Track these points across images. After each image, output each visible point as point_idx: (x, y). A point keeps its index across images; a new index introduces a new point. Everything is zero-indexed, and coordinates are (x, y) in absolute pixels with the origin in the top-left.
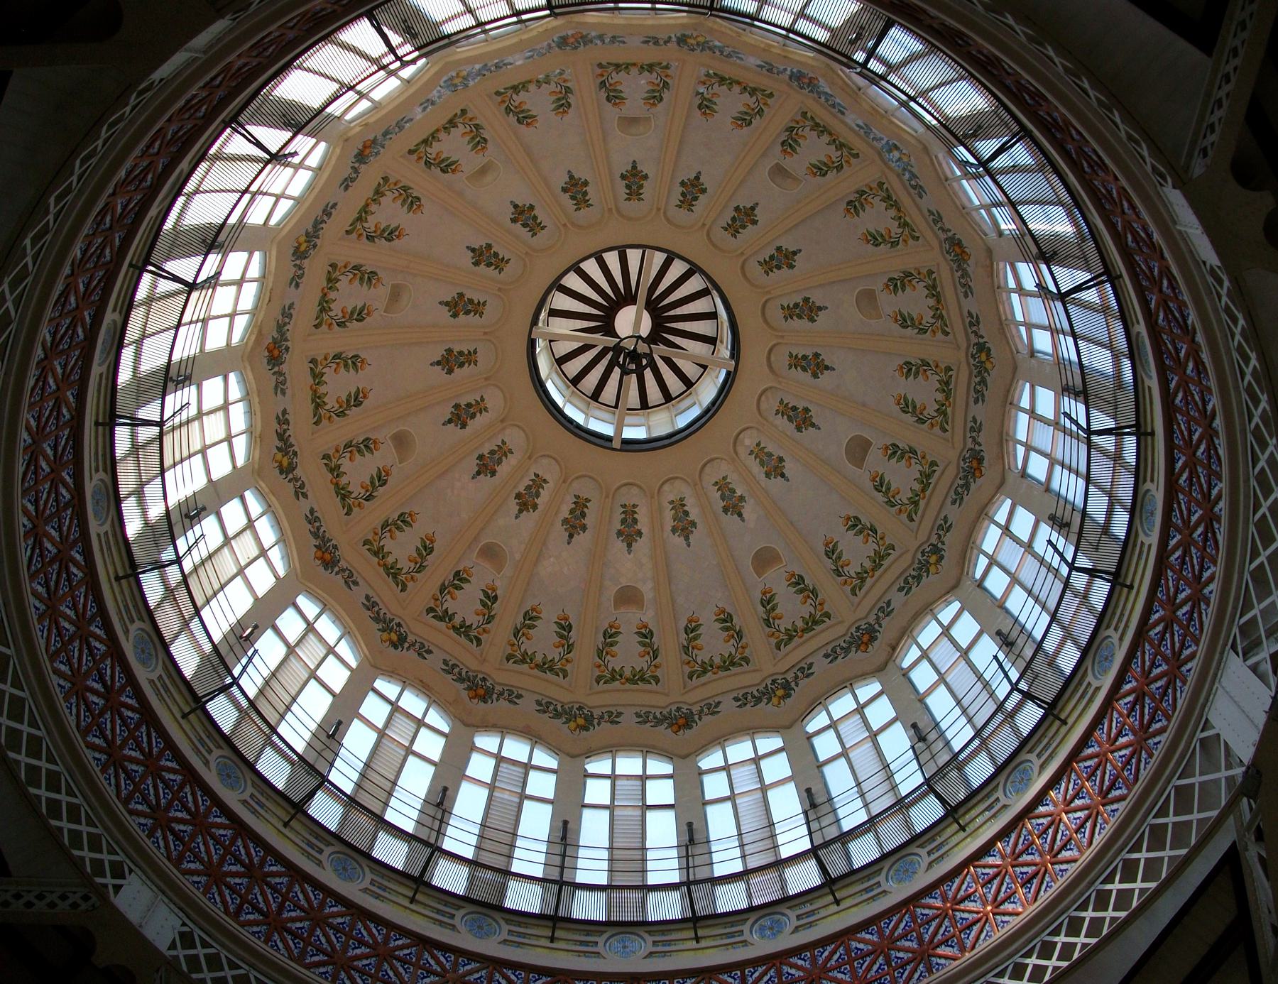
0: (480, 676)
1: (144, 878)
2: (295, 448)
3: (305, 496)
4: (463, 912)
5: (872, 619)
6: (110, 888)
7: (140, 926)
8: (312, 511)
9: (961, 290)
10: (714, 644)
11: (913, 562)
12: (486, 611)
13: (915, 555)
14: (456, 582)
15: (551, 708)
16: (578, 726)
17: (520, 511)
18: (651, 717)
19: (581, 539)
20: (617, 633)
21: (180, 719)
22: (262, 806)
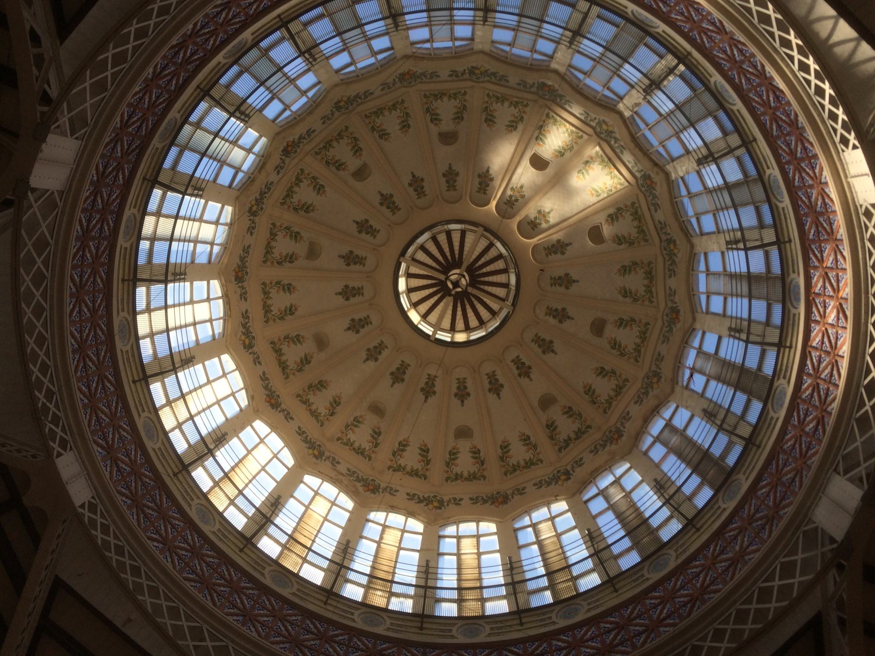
2: (432, 495)
3: (461, 500)
4: (720, 500)
8: (471, 499)
9: (434, 79)
14: (552, 429)
16: (657, 383)
17: (529, 377)
19: (557, 346)
21: (522, 628)
22: (598, 600)
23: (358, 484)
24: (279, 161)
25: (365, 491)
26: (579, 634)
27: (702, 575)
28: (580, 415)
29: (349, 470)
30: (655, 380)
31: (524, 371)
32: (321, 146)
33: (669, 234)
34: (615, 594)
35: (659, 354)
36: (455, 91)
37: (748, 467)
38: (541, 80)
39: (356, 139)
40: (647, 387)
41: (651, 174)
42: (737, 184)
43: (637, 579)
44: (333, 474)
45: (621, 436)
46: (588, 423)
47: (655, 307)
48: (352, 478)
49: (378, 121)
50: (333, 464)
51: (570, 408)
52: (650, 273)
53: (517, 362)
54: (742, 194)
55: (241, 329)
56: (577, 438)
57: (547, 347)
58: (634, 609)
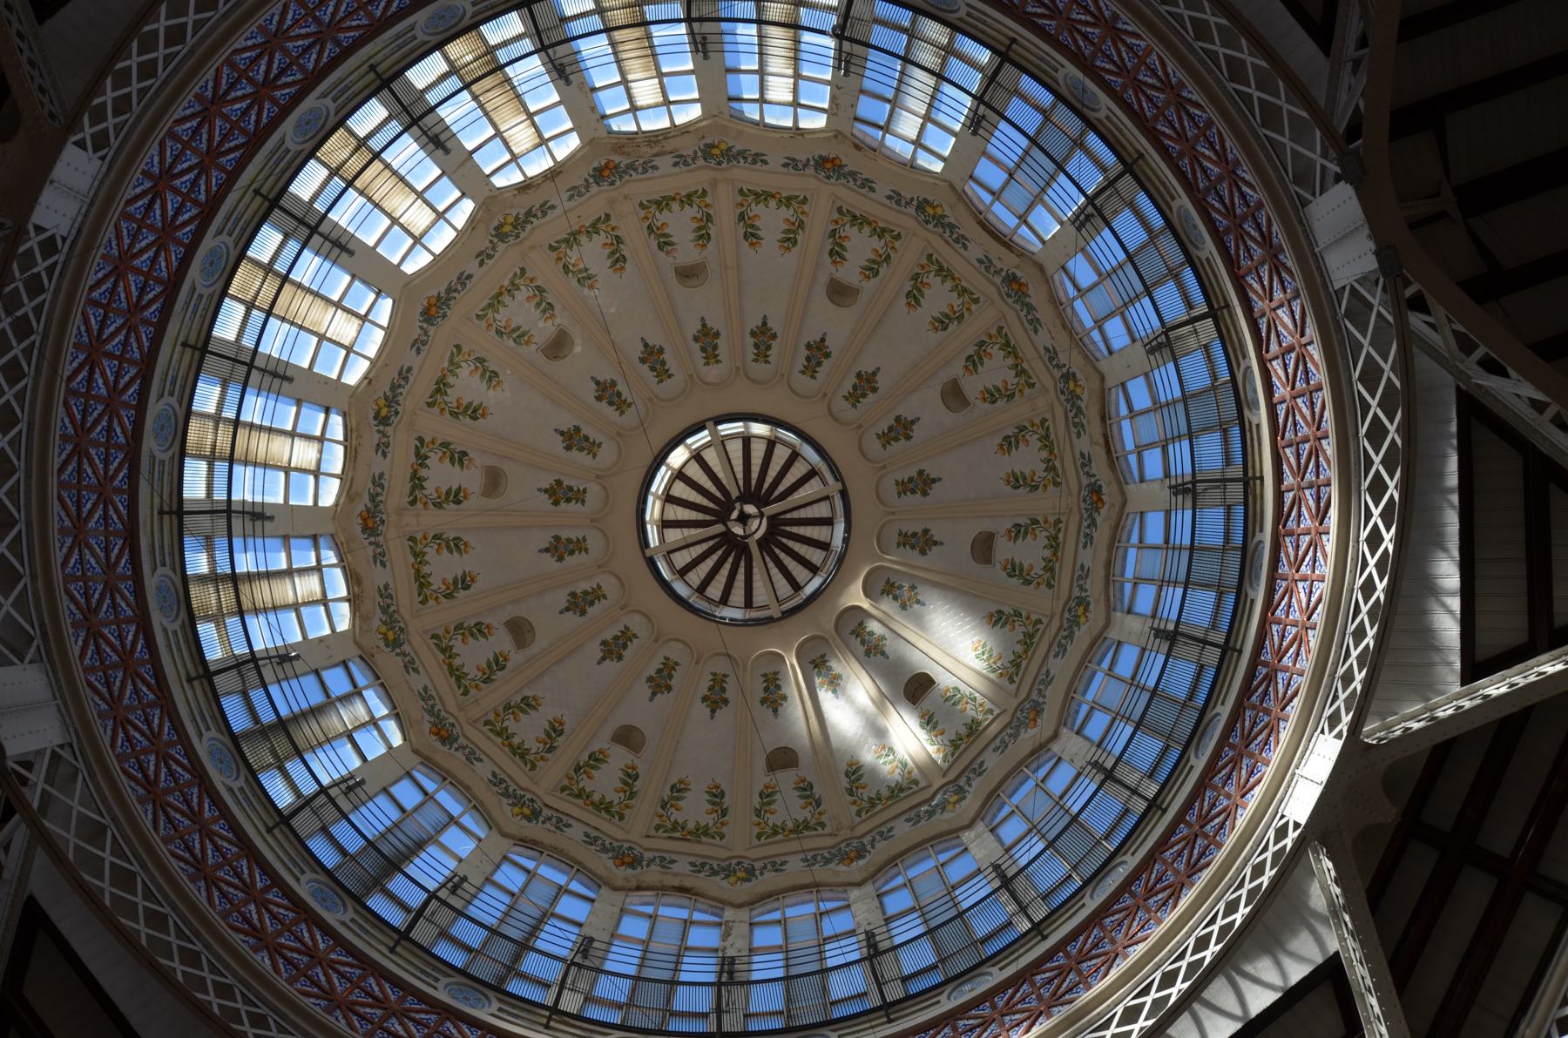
0: (384, 517)
1: (100, 176)
3: (482, 264)
5: (648, 855)
6: (79, 136)
7: (52, 182)
8: (470, 277)
11: (724, 860)
12: (443, 497)
13: (731, 858)
15: (388, 601)
16: (385, 634)
17: (546, 491)
18: (431, 702)
19: (549, 562)
20: (485, 636)
22: (194, 313)
23: (625, 161)
24: (1094, 471)
25: (609, 162)
26: (175, 253)
27: (101, 466)
28: (438, 505)
29: (655, 168)
30: (391, 635)
32: (1061, 536)
33: (543, 822)
34: (181, 339)
37: (178, 643)
38: (868, 857)
39: (1027, 582)
40: (391, 619)
41: (635, 872)
42: (517, 958)
43: (174, 382)
44: (669, 145)
45: (365, 529)
46: (419, 505)
48: (641, 161)
50: (681, 156)
51: (458, 502)
52: (522, 756)
53: (578, 496)
54: (503, 951)
55: (952, 220)
56: (414, 475)
58: (140, 347)
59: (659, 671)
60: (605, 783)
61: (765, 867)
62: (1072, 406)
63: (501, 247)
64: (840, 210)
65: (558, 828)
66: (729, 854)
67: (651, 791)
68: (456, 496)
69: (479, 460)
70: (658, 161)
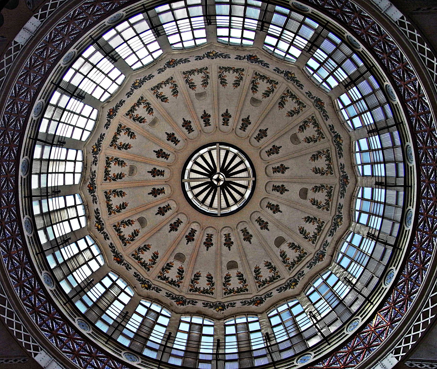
3: (108, 239)
8: (111, 244)
10: (266, 274)
11: (332, 224)
29: (95, 171)
30: (220, 308)
31: (190, 238)
32: (261, 74)
33: (299, 280)
35: (235, 303)
36: (322, 132)
47: (258, 290)
49: (288, 98)
50: (93, 162)
57: (208, 243)
59: (260, 224)
60: (292, 255)
61: (339, 211)
62: (218, 57)
63: (105, 230)
64: (127, 115)
65: (302, 276)
66: (330, 222)
67: (299, 240)
68: (181, 271)
69: (171, 260)
70: (93, 170)
